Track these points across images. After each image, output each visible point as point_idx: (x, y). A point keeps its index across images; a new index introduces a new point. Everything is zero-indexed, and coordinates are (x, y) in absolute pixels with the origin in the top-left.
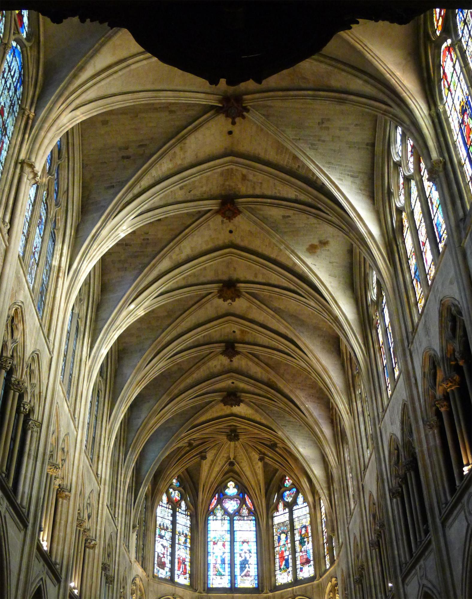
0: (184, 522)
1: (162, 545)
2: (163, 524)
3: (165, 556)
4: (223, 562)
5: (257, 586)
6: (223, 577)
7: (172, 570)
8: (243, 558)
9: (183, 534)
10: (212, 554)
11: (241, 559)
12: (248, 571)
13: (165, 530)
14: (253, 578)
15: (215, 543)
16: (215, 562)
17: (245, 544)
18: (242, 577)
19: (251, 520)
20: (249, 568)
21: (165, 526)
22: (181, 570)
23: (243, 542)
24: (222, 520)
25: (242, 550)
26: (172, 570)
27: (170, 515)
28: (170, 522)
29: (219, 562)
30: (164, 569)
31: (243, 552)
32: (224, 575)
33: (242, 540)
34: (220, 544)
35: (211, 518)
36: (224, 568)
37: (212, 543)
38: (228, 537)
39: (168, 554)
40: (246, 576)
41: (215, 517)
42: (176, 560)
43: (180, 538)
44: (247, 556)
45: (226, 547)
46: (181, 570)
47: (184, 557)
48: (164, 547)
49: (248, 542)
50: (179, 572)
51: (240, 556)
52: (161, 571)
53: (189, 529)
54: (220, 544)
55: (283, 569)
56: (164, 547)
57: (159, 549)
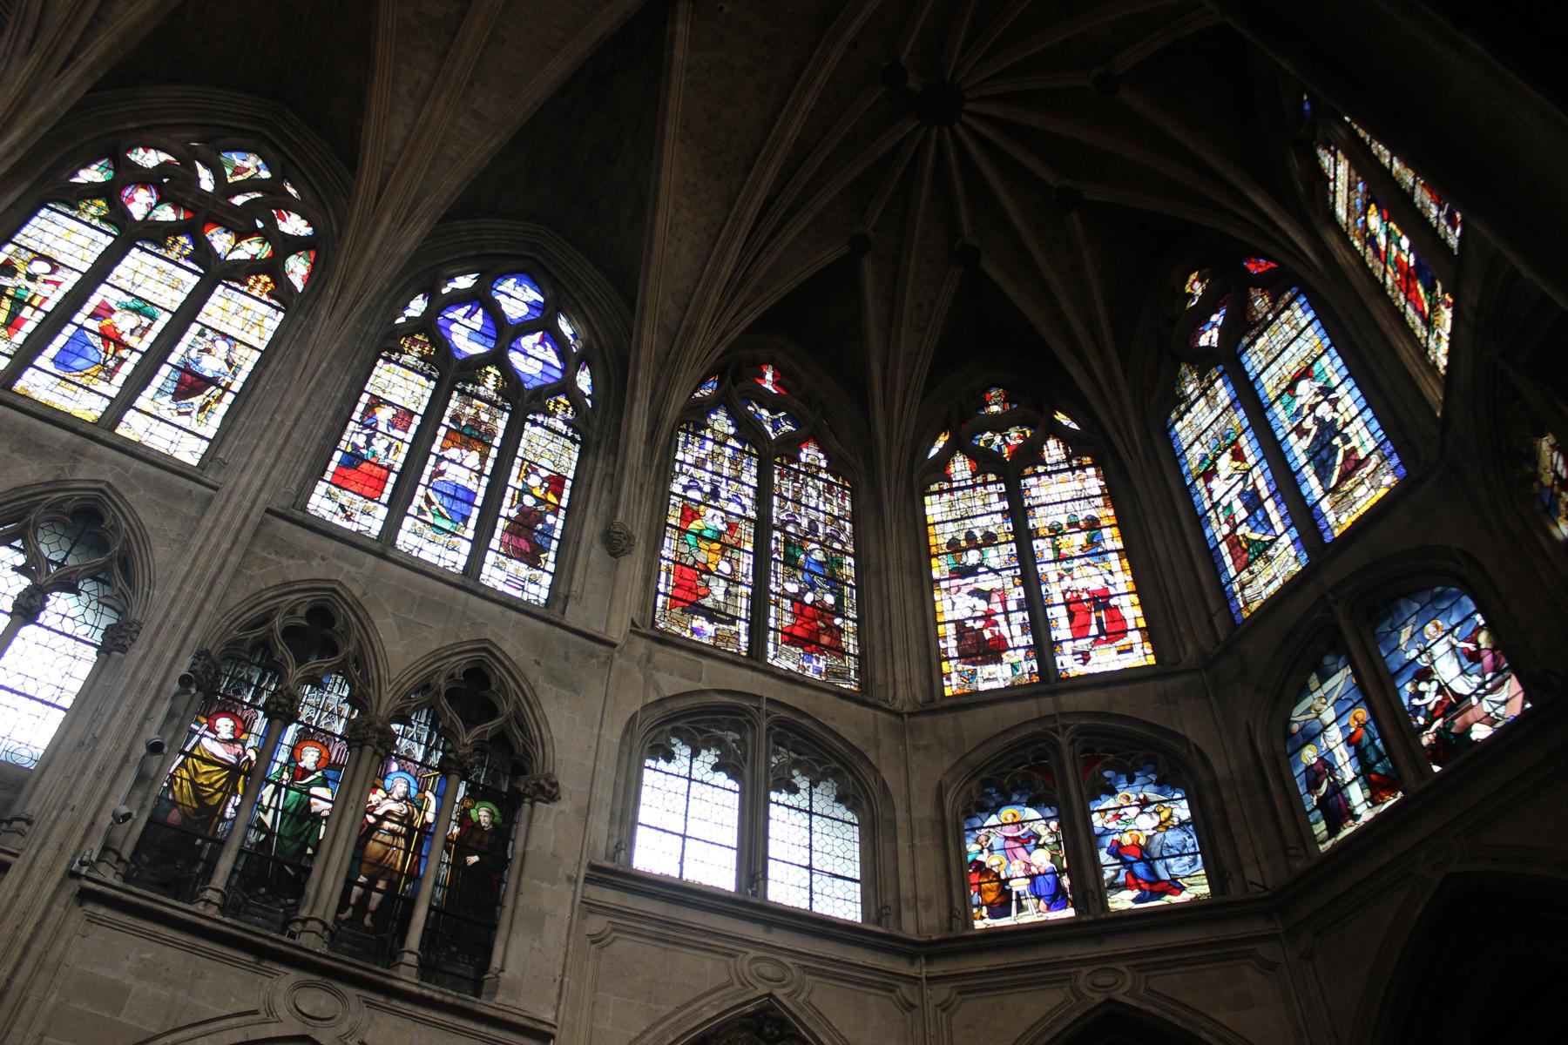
0: (1066, 492)
1: (977, 593)
2: (970, 536)
3: (1000, 619)
4: (1253, 501)
5: (1402, 471)
6: (1270, 553)
7: (1044, 648)
8: (1314, 430)
9: (1076, 524)
10: (1211, 514)
11: (1306, 442)
12: (1347, 455)
13: (978, 547)
14: (1374, 459)
15: (1209, 474)
16: (1226, 529)
17: (1304, 387)
18: (1335, 490)
19: (1287, 307)
20: (1346, 440)
21: (978, 534)
22: (1094, 630)
23: (1291, 388)
24: (1203, 394)
25: (1298, 413)
26: (1044, 648)
27: (995, 498)
28: (998, 518)
29: (1242, 514)
30: (999, 661)
31: (1306, 411)
32: (1272, 542)
33: (1283, 386)
34: (1225, 463)
35: (1174, 416)
36: (1266, 516)
37: (1200, 483)
38: (1239, 418)
39: (1012, 606)
40: (1345, 476)
41: (1183, 407)
42: (1059, 614)
43: (1063, 540)
44: (1324, 410)
45: (1246, 451)
46: (1094, 630)
47: (1096, 584)
48: (985, 595)
49: (1306, 373)
50: (1082, 644)
51: (1301, 432)
52: (985, 670)
53: (1099, 501)
54: (1225, 463)
55: (1431, 310)
56: (985, 595)
57: (955, 605)
